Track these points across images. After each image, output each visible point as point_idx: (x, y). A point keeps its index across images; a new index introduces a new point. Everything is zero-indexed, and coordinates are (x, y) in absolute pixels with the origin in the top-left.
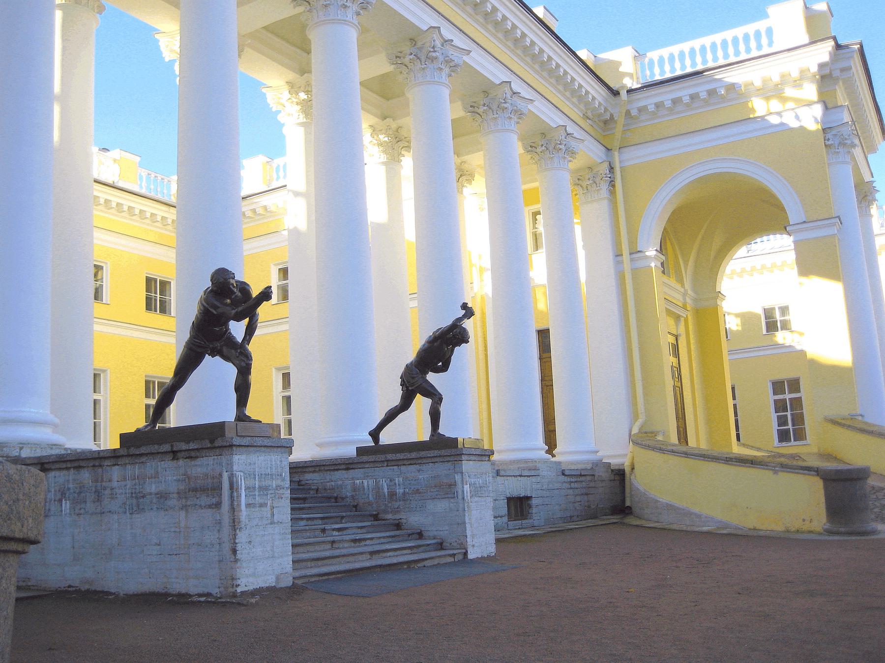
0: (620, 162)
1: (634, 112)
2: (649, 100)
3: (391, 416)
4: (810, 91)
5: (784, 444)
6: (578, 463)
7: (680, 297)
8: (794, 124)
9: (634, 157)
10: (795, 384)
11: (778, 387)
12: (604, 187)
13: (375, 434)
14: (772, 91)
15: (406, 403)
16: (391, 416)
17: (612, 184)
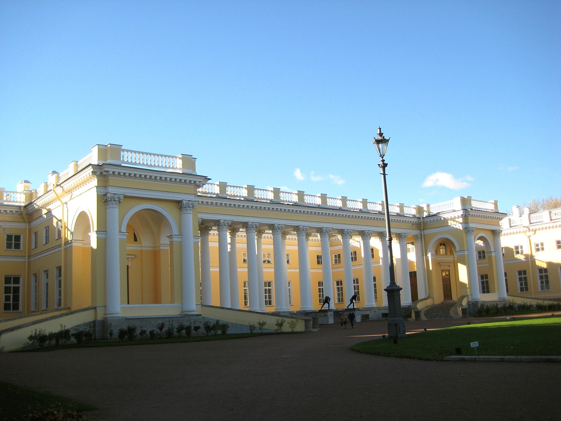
0: (423, 233)
1: (425, 222)
2: (428, 219)
3: (349, 305)
4: (461, 220)
5: (543, 290)
6: (407, 305)
7: (453, 259)
8: (458, 228)
9: (427, 232)
10: (525, 272)
11: (520, 273)
12: (420, 240)
13: (348, 307)
14: (453, 219)
15: (351, 304)
16: (349, 305)
17: (422, 238)
